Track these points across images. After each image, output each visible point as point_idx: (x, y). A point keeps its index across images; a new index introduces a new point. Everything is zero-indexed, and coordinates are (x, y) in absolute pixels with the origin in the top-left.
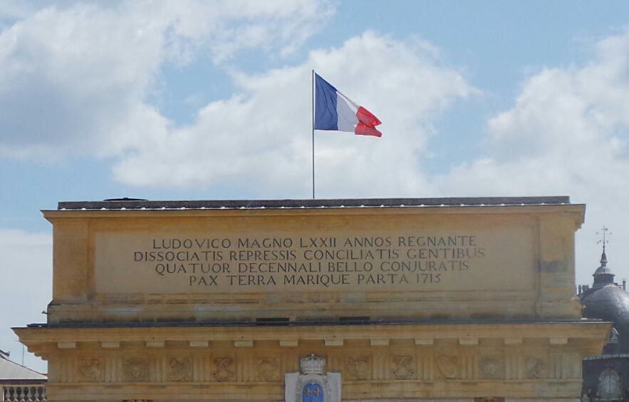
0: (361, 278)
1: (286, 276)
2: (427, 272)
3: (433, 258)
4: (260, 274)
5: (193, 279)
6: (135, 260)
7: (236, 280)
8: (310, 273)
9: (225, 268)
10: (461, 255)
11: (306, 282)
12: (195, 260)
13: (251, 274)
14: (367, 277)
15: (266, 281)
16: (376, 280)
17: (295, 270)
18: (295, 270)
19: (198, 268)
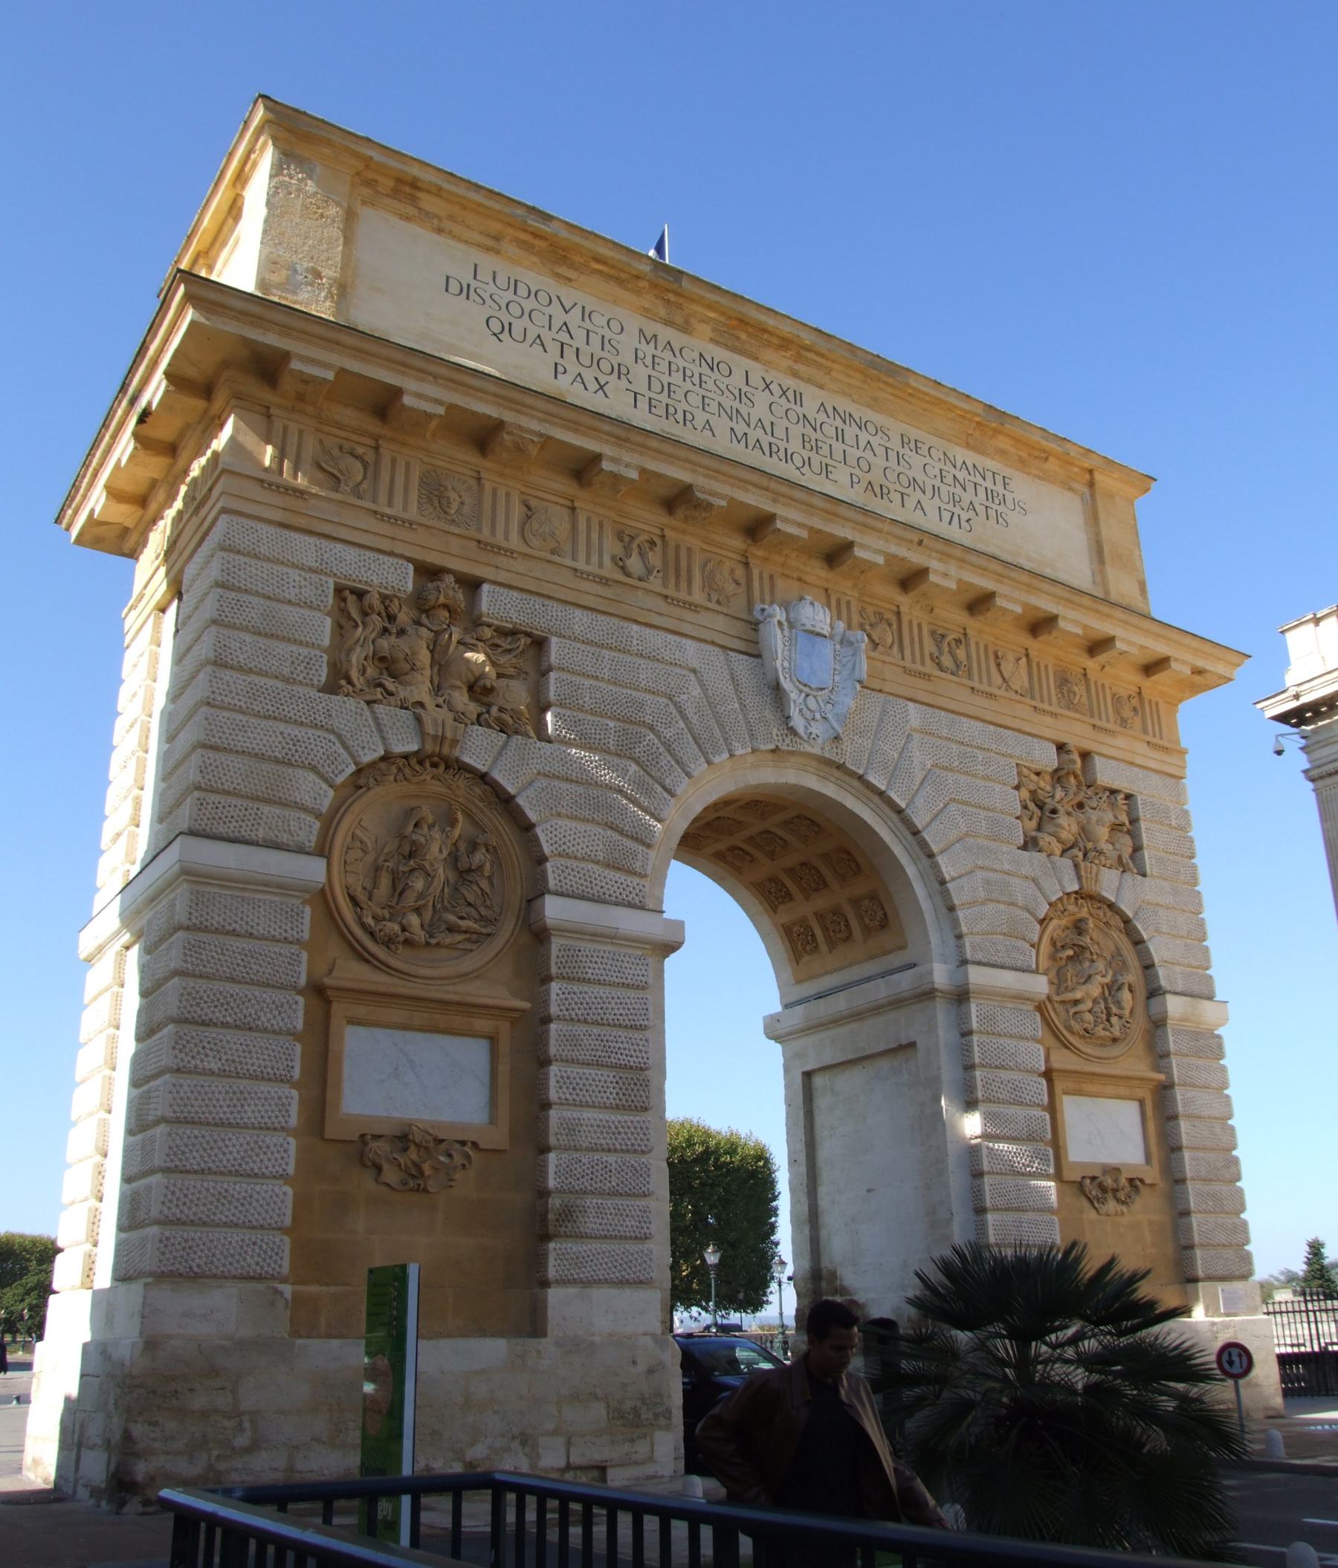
0: (855, 480)
1: (732, 429)
2: (950, 507)
3: (958, 490)
4: (684, 406)
5: (560, 369)
6: (447, 290)
7: (643, 404)
8: (772, 440)
9: (619, 371)
10: (996, 501)
11: (767, 452)
12: (564, 337)
13: (670, 402)
14: (863, 484)
15: (699, 422)
16: (877, 490)
17: (749, 425)
18: (749, 425)
19: (569, 353)
